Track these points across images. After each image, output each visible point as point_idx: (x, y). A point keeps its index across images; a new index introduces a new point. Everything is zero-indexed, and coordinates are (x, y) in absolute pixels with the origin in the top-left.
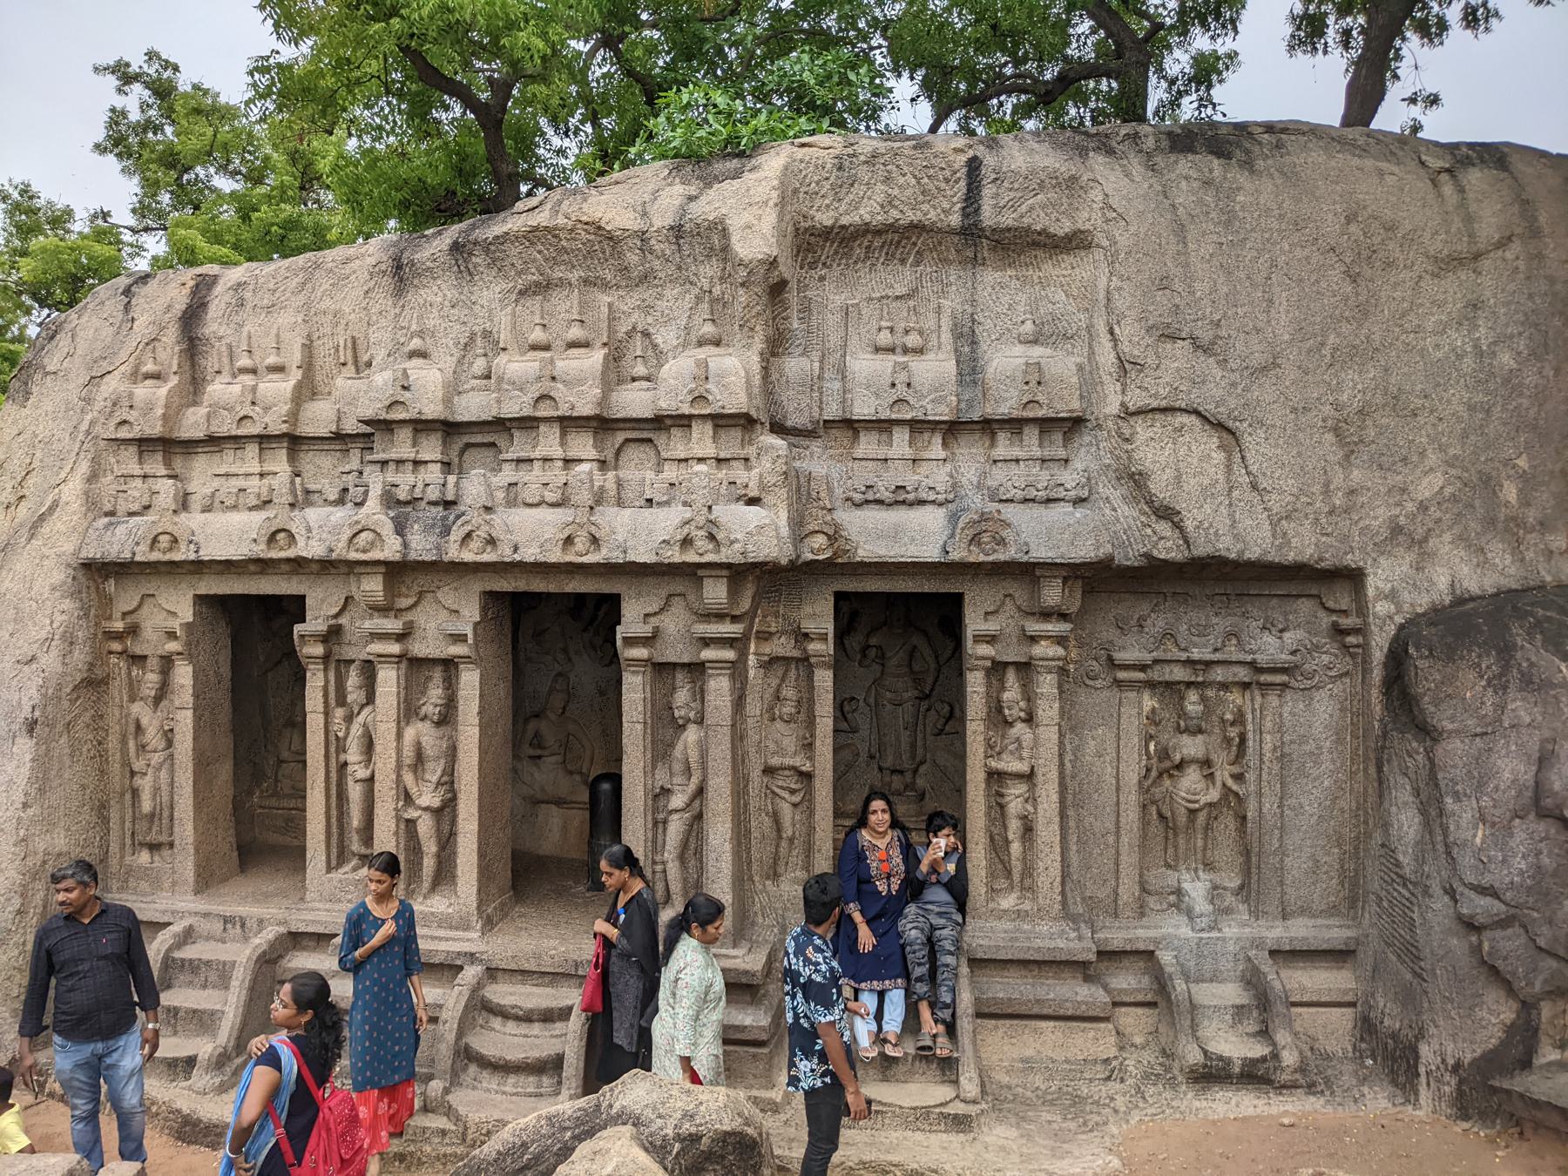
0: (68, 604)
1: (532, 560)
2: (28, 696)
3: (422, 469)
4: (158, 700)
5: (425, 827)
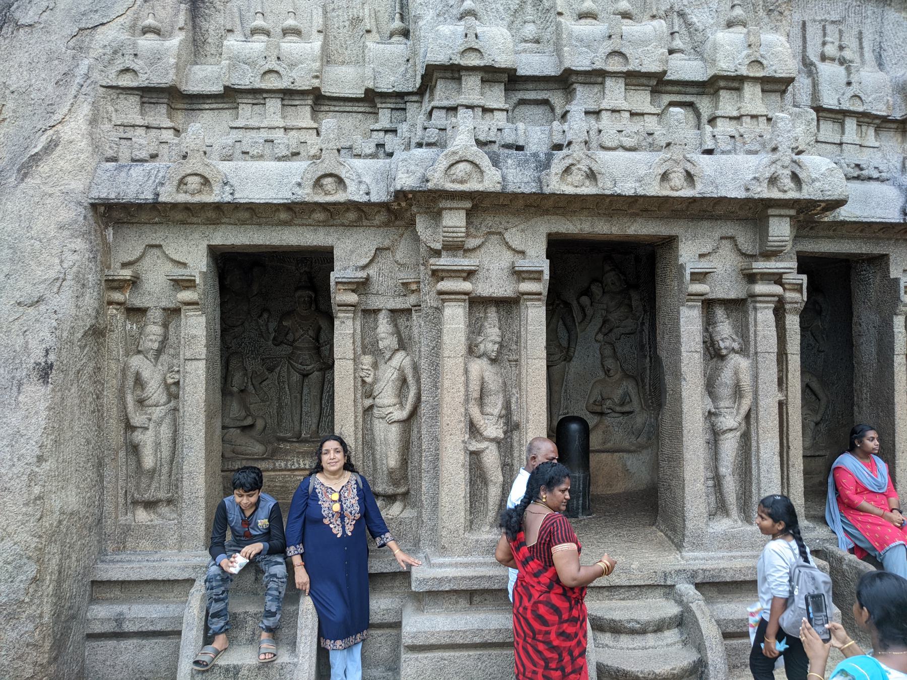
0: (80, 244)
1: (631, 193)
2: (39, 339)
3: (488, 116)
4: (159, 352)
5: (491, 458)
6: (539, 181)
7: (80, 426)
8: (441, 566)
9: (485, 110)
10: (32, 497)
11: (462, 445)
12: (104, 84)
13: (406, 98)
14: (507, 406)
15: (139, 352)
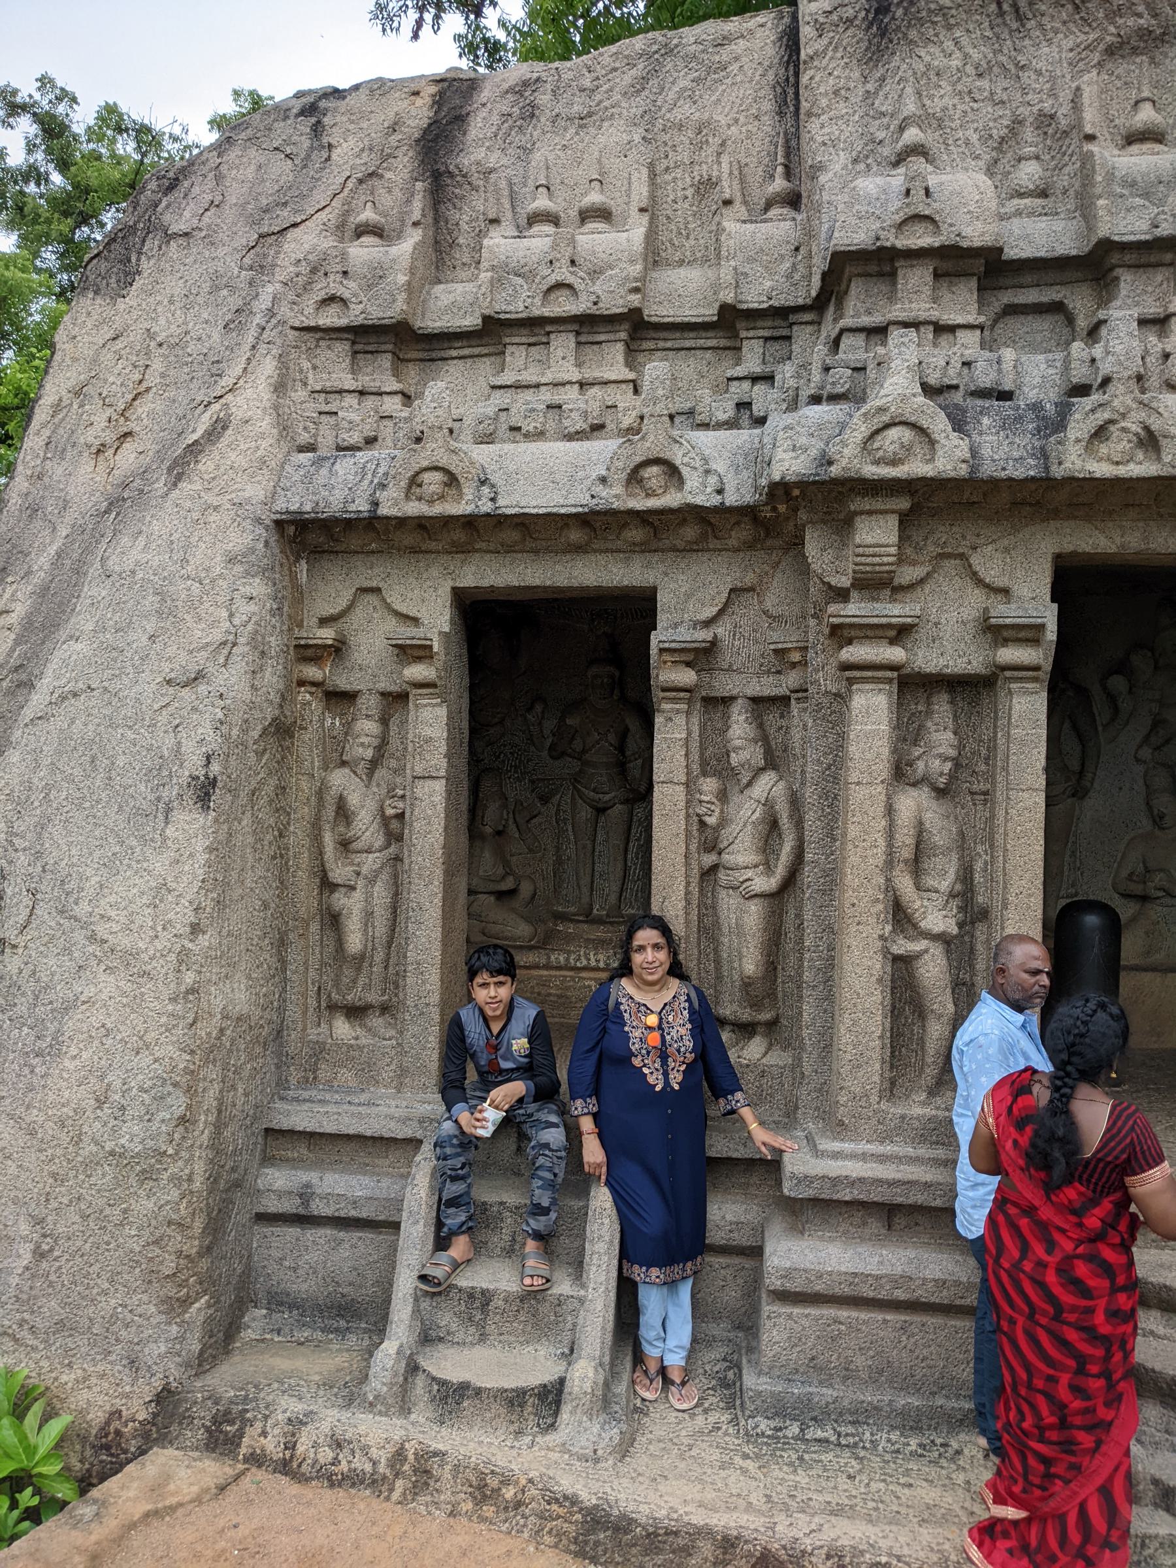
0: (258, 587)
2: (197, 739)
3: (944, 339)
4: (374, 764)
5: (933, 969)
6: (1044, 454)
7: (254, 877)
8: (836, 1155)
9: (942, 329)
10: (183, 988)
11: (879, 944)
12: (297, 324)
13: (792, 318)
14: (966, 876)
15: (344, 764)
